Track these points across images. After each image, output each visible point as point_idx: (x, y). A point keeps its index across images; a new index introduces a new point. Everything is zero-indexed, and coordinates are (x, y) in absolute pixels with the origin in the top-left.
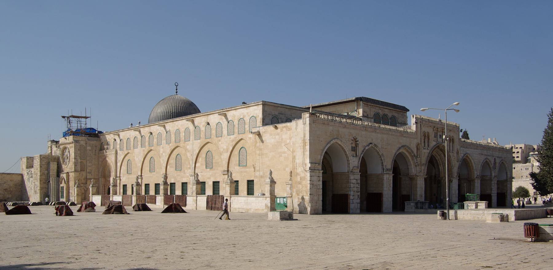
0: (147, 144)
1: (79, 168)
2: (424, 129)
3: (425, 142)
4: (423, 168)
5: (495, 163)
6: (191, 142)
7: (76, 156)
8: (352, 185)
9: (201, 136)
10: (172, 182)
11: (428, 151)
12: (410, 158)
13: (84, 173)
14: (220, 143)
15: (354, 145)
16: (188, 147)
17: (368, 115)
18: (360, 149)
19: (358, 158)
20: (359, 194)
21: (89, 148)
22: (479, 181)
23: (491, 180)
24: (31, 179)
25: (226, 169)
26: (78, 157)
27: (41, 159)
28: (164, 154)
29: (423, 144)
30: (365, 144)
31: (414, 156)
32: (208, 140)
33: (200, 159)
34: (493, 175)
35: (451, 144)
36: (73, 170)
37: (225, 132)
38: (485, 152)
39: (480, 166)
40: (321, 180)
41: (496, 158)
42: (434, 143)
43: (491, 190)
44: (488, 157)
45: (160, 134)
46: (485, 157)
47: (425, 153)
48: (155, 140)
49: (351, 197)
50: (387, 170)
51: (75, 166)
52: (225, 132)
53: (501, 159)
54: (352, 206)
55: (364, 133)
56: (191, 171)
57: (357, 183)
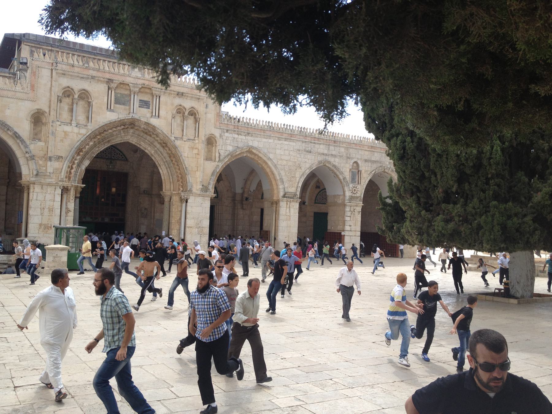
2: (65, 82)
3: (71, 110)
5: (356, 173)
11: (83, 131)
22: (297, 206)
29: (65, 115)
34: (348, 194)
35: (190, 121)
38: (322, 148)
39: (298, 175)
41: (359, 162)
42: (111, 117)
43: (344, 225)
44: (332, 160)
46: (320, 158)
53: (375, 166)
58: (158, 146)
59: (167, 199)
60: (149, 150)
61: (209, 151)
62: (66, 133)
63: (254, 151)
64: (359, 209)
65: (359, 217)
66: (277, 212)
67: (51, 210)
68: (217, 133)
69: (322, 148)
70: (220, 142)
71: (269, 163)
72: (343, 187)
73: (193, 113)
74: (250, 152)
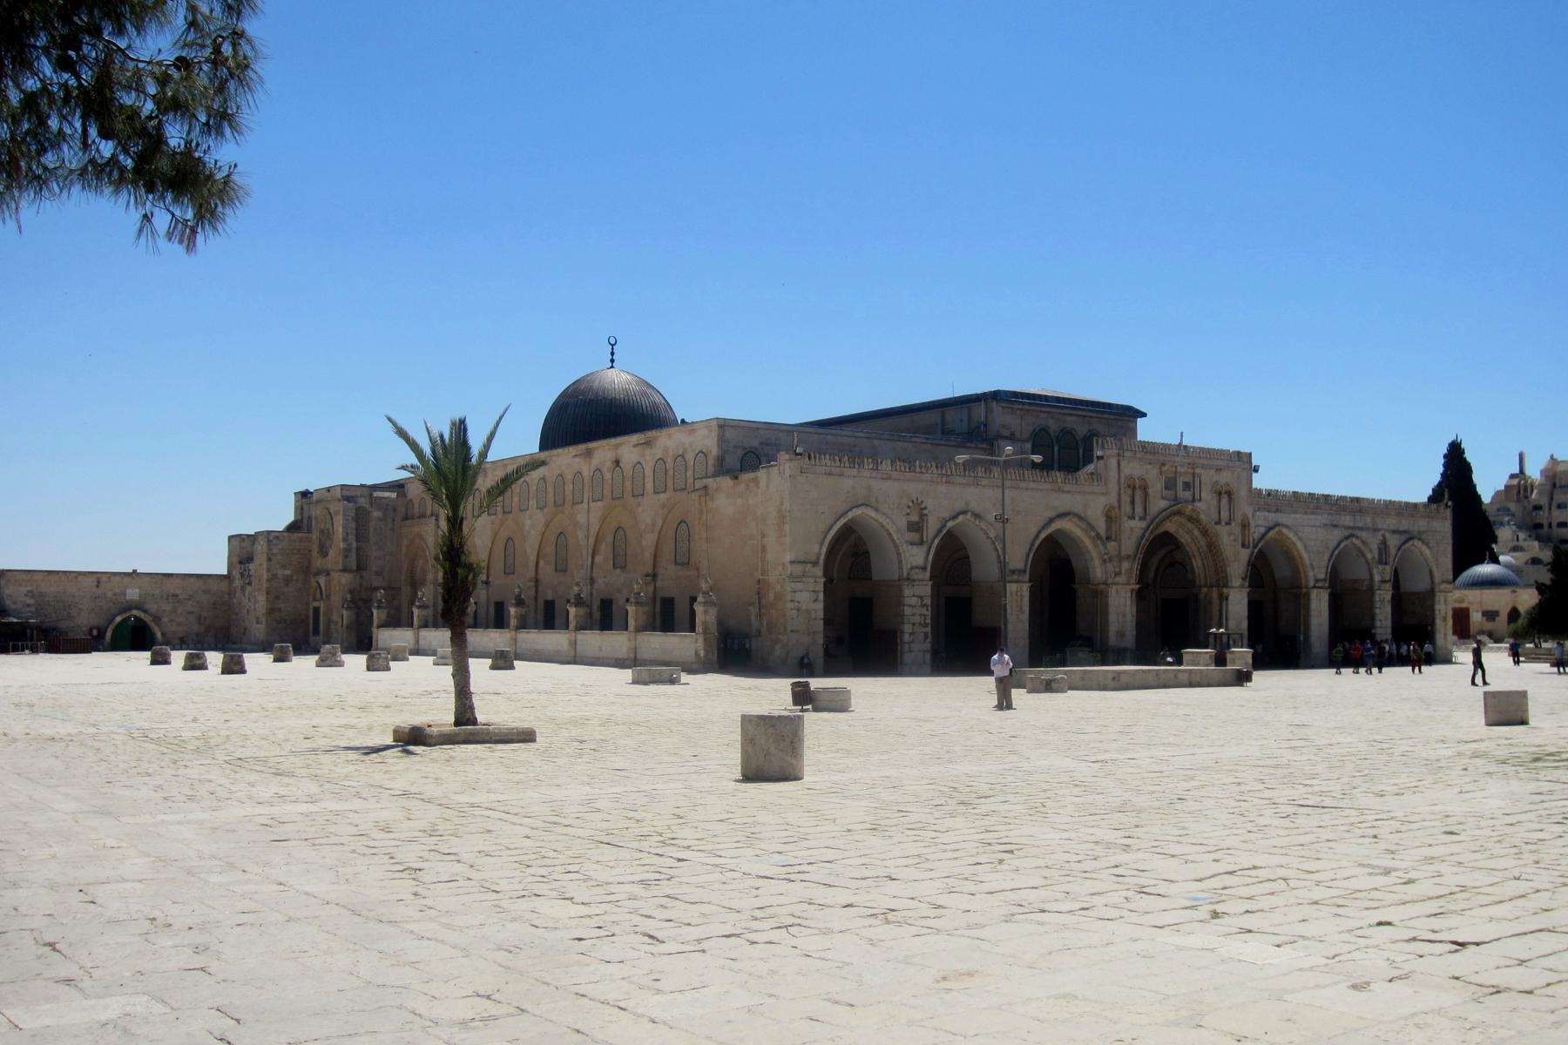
1: (353, 564)
3: (1133, 502)
4: (1125, 565)
6: (585, 506)
8: (908, 611)
10: (549, 598)
11: (1144, 524)
12: (1087, 542)
13: (364, 573)
15: (915, 518)
17: (1013, 434)
18: (932, 525)
19: (925, 548)
20: (928, 629)
21: (377, 514)
23: (1371, 591)
24: (249, 589)
26: (352, 538)
27: (269, 541)
30: (946, 515)
31: (1098, 536)
34: (1377, 578)
35: (1225, 501)
37: (649, 486)
38: (1347, 520)
40: (821, 596)
44: (1359, 533)
46: (1346, 533)
47: (1133, 530)
49: (907, 638)
50: (1013, 572)
52: (649, 486)
53: (1404, 537)
54: (908, 658)
55: (942, 488)
57: (923, 606)
58: (1196, 532)
59: (1202, 596)
60: (1184, 538)
61: (1243, 535)
62: (1132, 529)
63: (1285, 531)
64: (1388, 596)
65: (1389, 609)
66: (1308, 608)
67: (1124, 615)
68: (1249, 511)
69: (1347, 520)
70: (1252, 524)
71: (1299, 545)
72: (1370, 571)
73: (1229, 494)
74: (1280, 533)
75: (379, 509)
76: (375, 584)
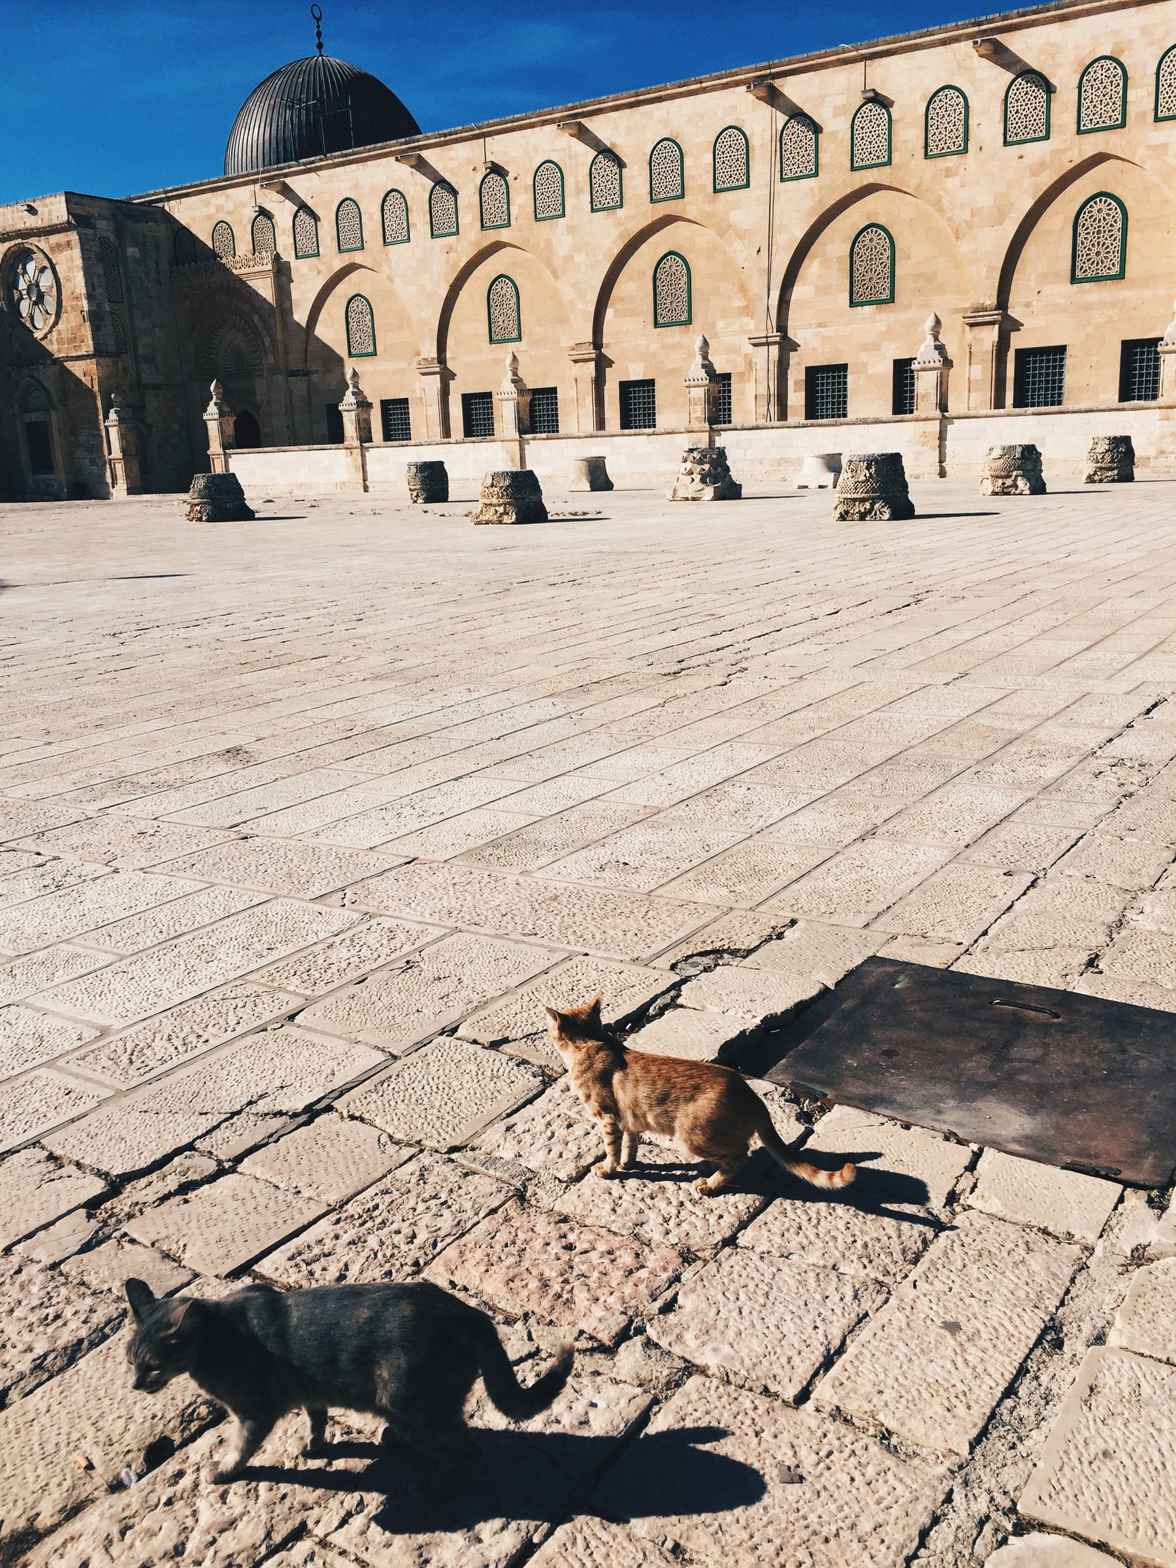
0: (468, 218)
7: (90, 284)
9: (824, 159)
14: (952, 183)
16: (735, 217)
21: (132, 251)
25: (991, 300)
26: (99, 291)
28: (579, 258)
32: (870, 177)
33: (811, 268)
36: (91, 349)
45: (550, 173)
48: (521, 201)
51: (95, 330)
56: (762, 324)
75: (135, 243)
76: (146, 379)
